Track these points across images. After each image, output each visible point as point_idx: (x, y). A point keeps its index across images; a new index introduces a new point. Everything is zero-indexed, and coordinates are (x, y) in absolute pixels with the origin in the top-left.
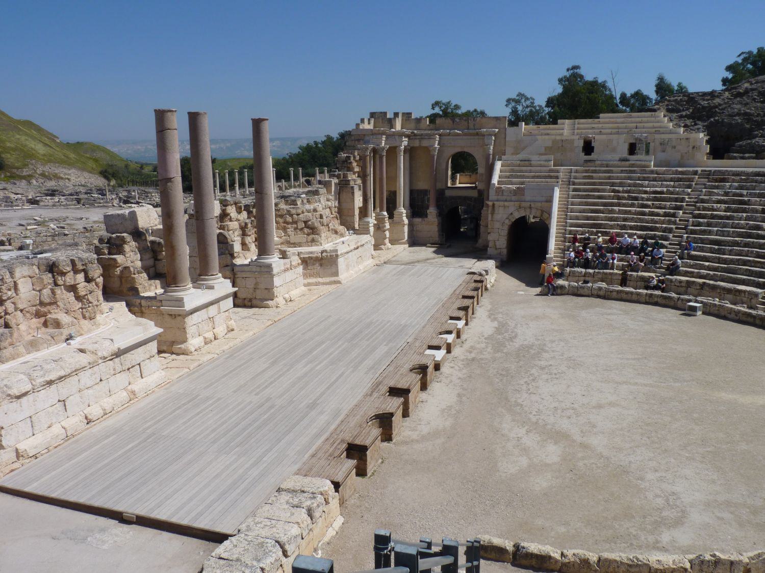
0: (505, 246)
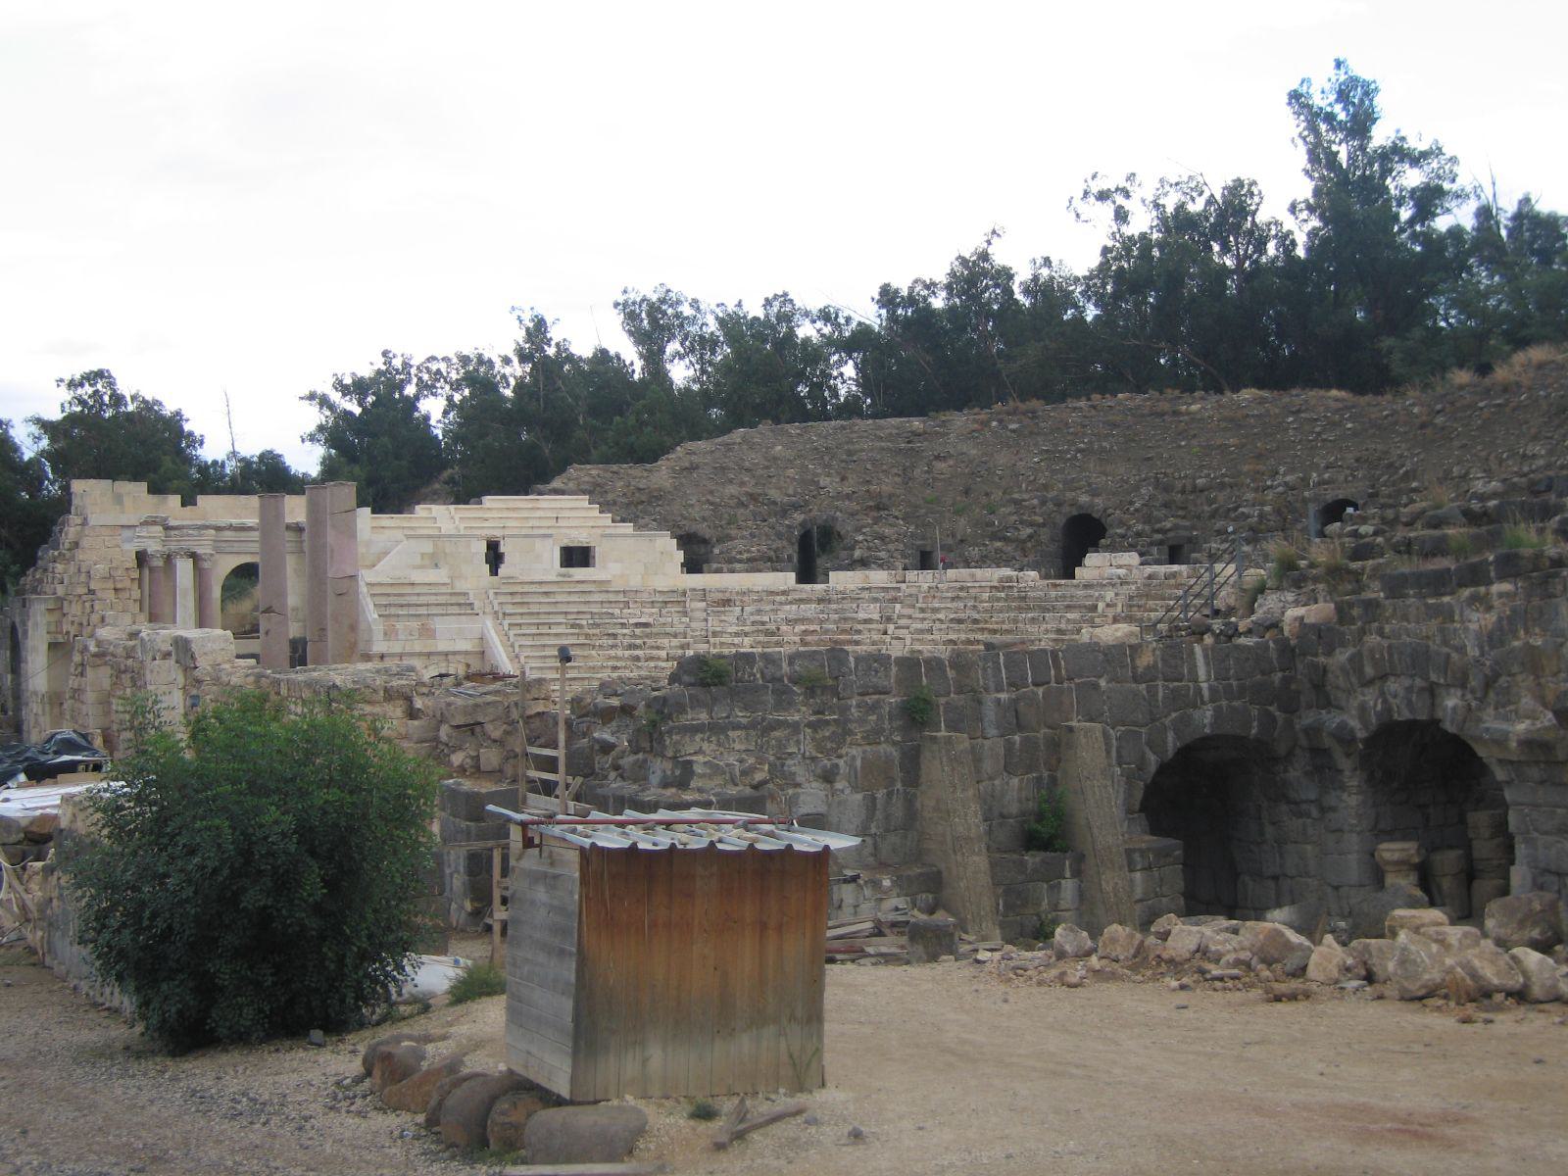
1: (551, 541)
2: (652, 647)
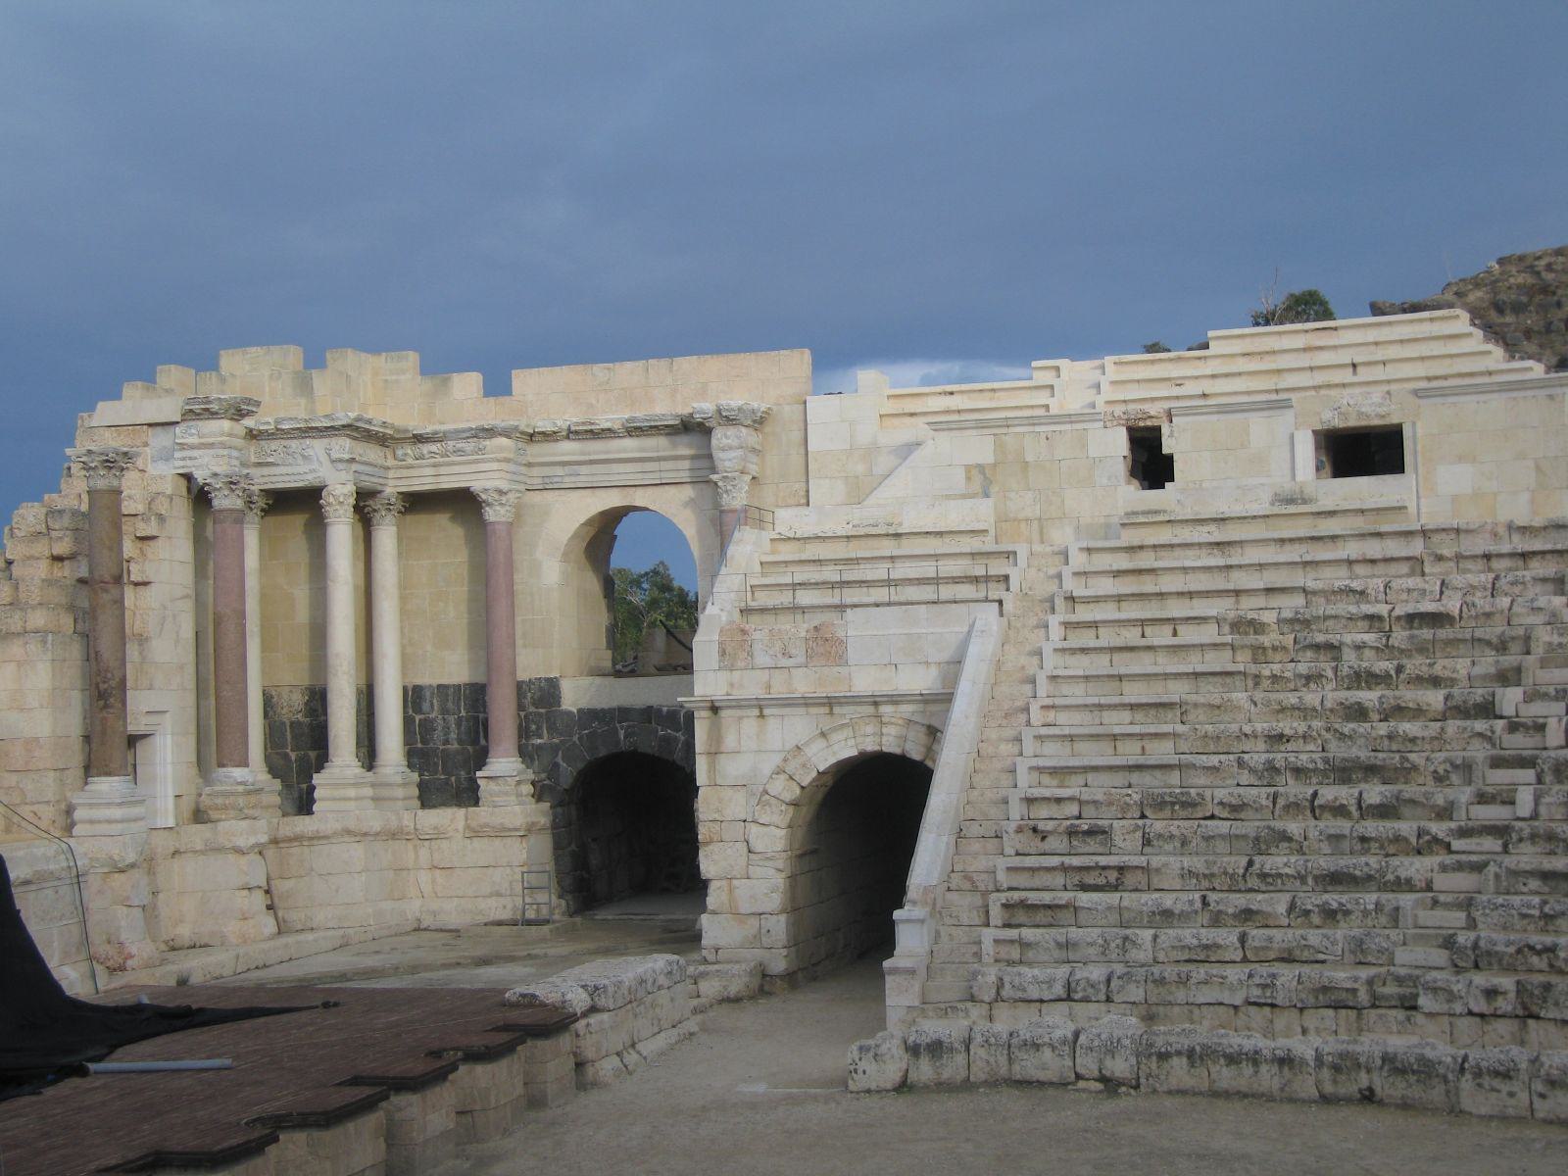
0: (776, 901)
1: (1288, 416)
2: (1419, 680)
